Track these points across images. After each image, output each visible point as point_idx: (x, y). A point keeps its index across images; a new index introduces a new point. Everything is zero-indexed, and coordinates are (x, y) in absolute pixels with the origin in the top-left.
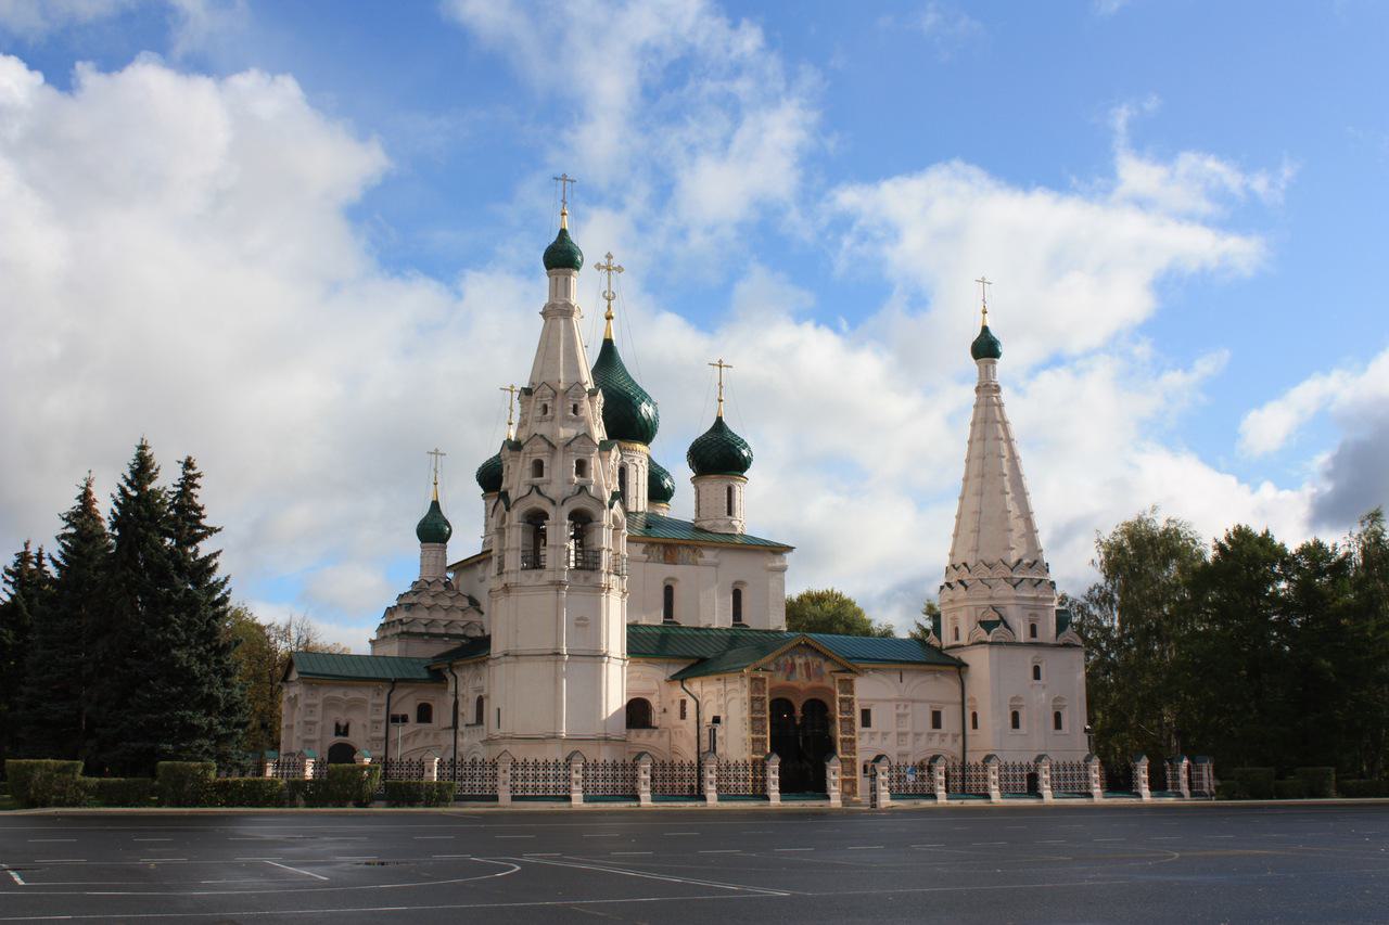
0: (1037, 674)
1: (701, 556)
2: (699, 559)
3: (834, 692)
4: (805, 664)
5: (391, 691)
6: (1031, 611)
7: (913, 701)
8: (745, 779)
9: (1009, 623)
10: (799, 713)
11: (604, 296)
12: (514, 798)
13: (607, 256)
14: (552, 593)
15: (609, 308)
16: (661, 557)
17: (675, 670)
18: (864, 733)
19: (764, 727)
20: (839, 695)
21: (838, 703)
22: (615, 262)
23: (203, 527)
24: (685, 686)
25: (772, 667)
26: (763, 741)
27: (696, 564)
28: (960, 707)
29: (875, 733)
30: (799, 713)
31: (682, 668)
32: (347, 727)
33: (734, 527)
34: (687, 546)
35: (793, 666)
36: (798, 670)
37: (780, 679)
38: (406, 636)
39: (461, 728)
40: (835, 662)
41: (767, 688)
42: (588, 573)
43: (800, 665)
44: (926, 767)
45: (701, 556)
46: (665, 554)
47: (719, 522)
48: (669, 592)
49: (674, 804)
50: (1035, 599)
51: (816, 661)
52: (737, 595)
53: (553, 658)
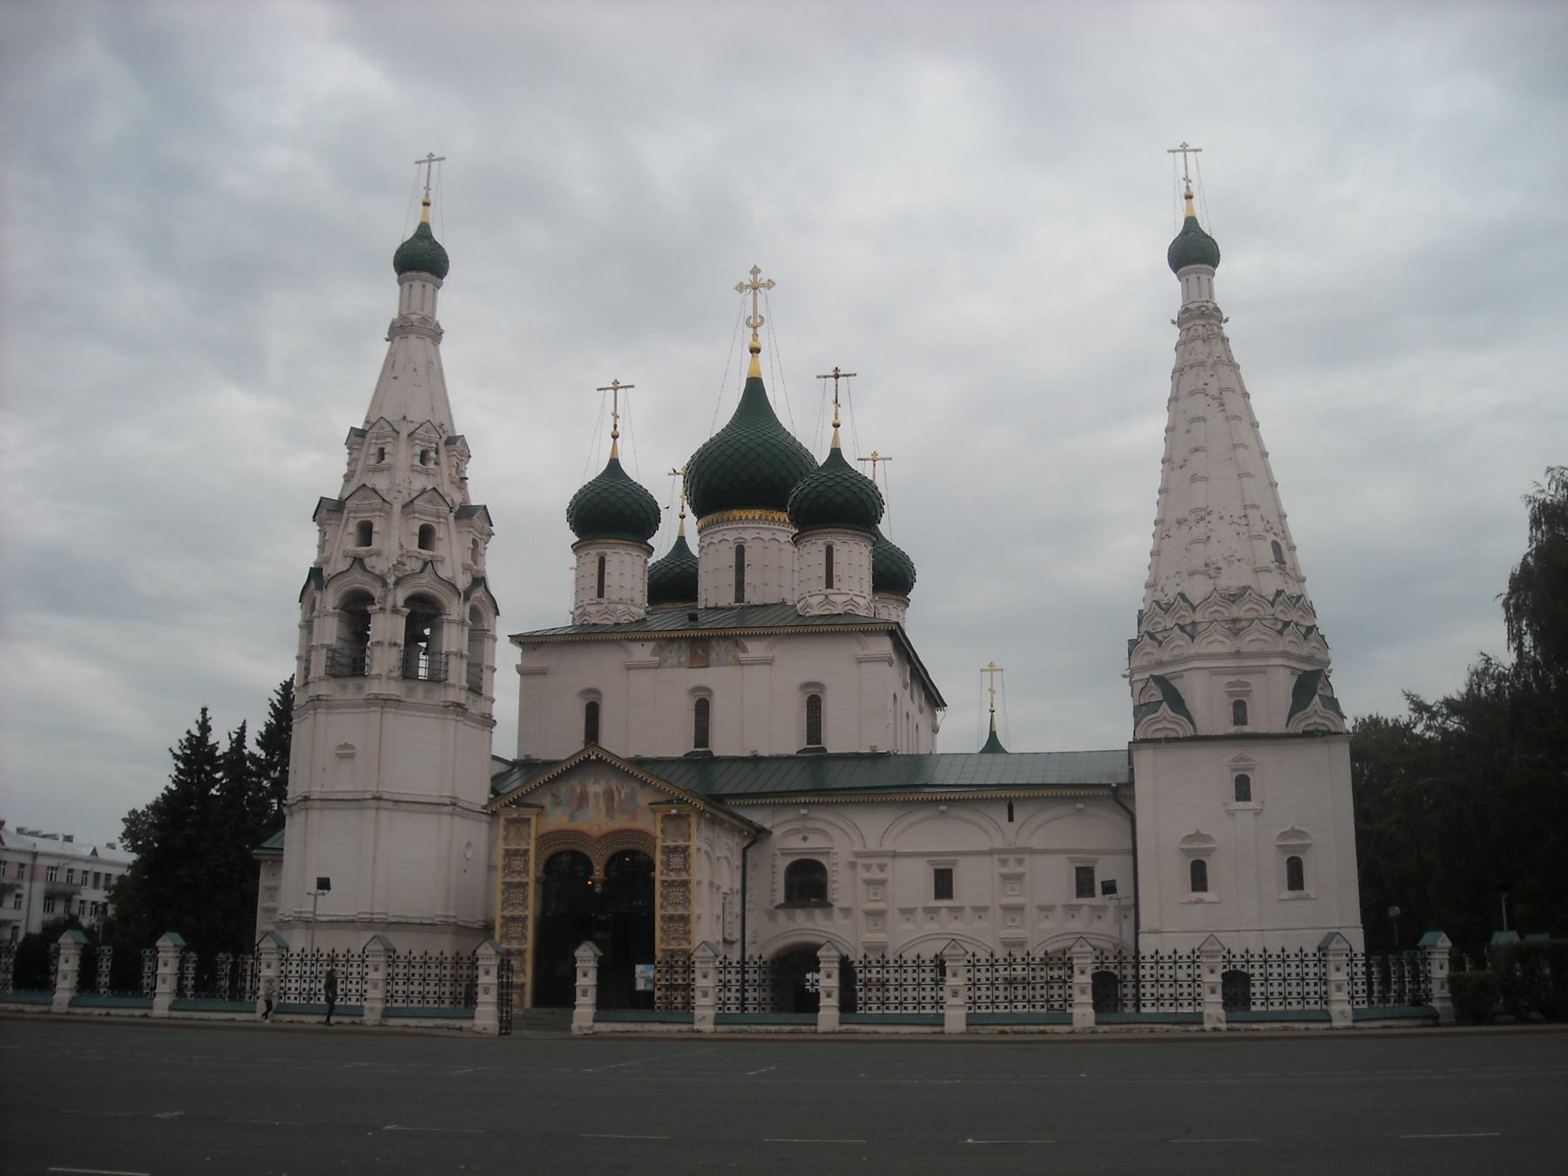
0: (1243, 789)
1: (745, 650)
2: (742, 656)
3: (654, 839)
4: (605, 793)
6: (1233, 679)
7: (1032, 851)
8: (424, 980)
9: (1187, 704)
10: (598, 872)
11: (748, 323)
13: (751, 272)
15: (755, 336)
16: (682, 659)
18: (936, 910)
19: (525, 898)
20: (659, 844)
21: (659, 858)
22: (763, 277)
25: (547, 801)
26: (524, 919)
27: (740, 664)
28: (1130, 857)
29: (960, 909)
30: (598, 872)
33: (834, 603)
34: (725, 637)
35: (583, 798)
36: (592, 801)
37: (557, 819)
40: (658, 790)
41: (533, 834)
42: (358, 681)
43: (596, 795)
44: (1062, 961)
45: (745, 650)
46: (693, 655)
48: (703, 709)
50: (1238, 654)
51: (623, 790)
52: (814, 706)
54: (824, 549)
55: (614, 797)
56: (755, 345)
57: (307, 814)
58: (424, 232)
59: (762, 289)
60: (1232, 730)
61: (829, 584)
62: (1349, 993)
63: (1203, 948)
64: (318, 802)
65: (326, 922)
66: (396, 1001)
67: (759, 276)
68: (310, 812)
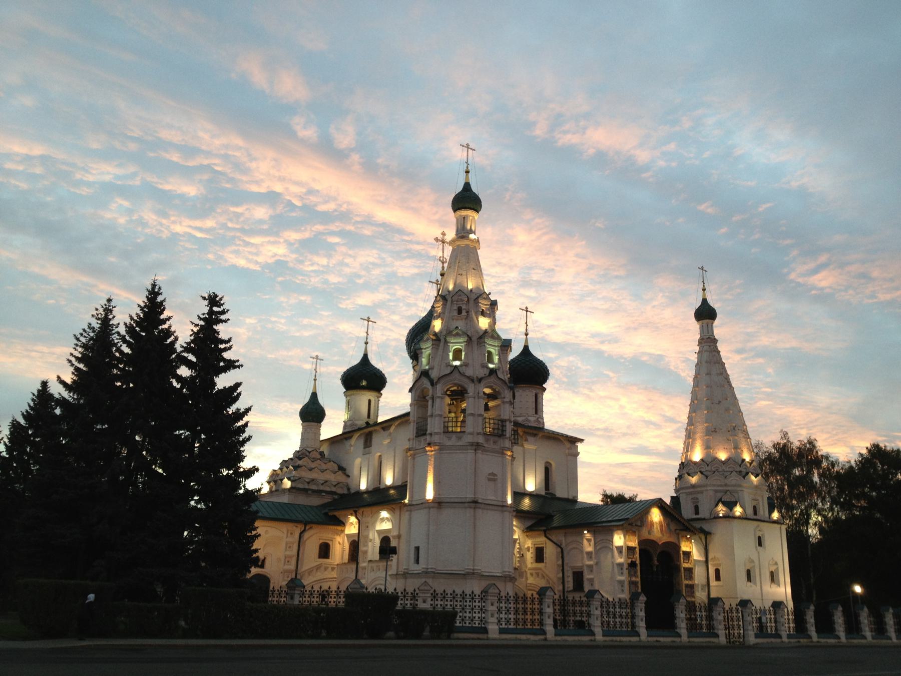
0: (760, 542)
4: (659, 522)
5: (304, 530)
12: (502, 631)
14: (471, 452)
17: (529, 523)
23: (224, 360)
24: (548, 535)
31: (531, 523)
32: (265, 558)
38: (294, 491)
39: (362, 564)
43: (656, 523)
47: (530, 418)
49: (580, 638)
53: (473, 505)
54: (534, 394)
55: (662, 526)
56: (443, 272)
57: (475, 512)
58: (467, 187)
59: (446, 244)
60: (753, 516)
61: (536, 413)
62: (497, 618)
63: (421, 588)
64: (483, 505)
65: (488, 576)
66: (510, 624)
67: (445, 237)
68: (477, 510)
